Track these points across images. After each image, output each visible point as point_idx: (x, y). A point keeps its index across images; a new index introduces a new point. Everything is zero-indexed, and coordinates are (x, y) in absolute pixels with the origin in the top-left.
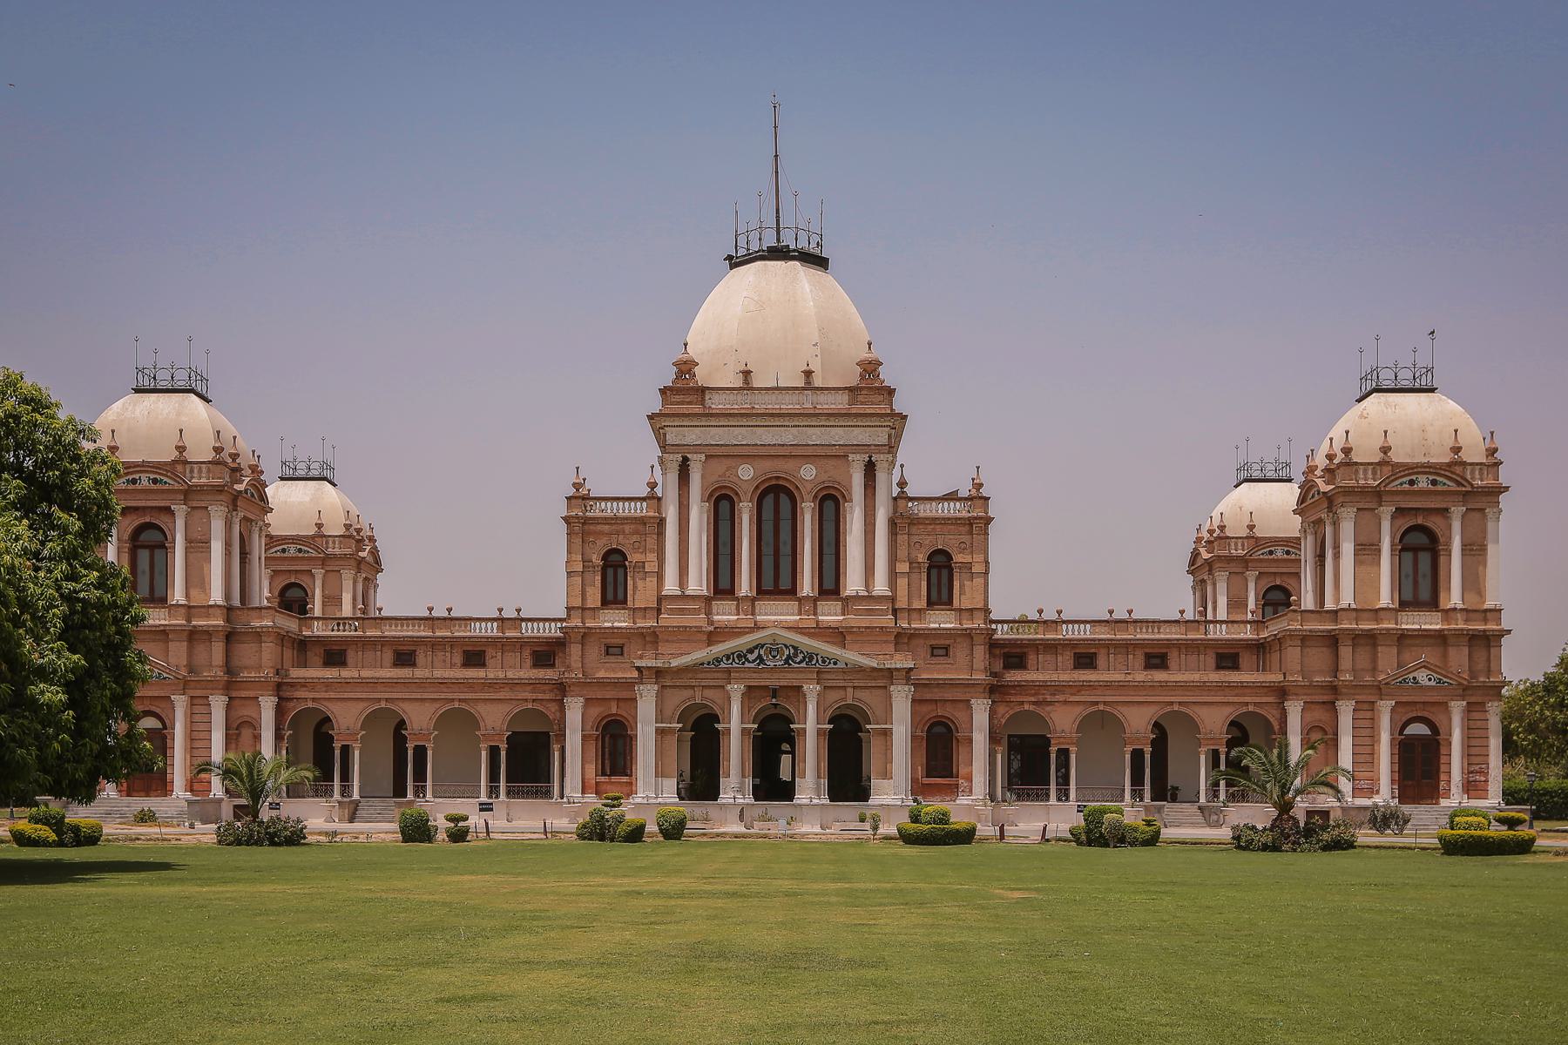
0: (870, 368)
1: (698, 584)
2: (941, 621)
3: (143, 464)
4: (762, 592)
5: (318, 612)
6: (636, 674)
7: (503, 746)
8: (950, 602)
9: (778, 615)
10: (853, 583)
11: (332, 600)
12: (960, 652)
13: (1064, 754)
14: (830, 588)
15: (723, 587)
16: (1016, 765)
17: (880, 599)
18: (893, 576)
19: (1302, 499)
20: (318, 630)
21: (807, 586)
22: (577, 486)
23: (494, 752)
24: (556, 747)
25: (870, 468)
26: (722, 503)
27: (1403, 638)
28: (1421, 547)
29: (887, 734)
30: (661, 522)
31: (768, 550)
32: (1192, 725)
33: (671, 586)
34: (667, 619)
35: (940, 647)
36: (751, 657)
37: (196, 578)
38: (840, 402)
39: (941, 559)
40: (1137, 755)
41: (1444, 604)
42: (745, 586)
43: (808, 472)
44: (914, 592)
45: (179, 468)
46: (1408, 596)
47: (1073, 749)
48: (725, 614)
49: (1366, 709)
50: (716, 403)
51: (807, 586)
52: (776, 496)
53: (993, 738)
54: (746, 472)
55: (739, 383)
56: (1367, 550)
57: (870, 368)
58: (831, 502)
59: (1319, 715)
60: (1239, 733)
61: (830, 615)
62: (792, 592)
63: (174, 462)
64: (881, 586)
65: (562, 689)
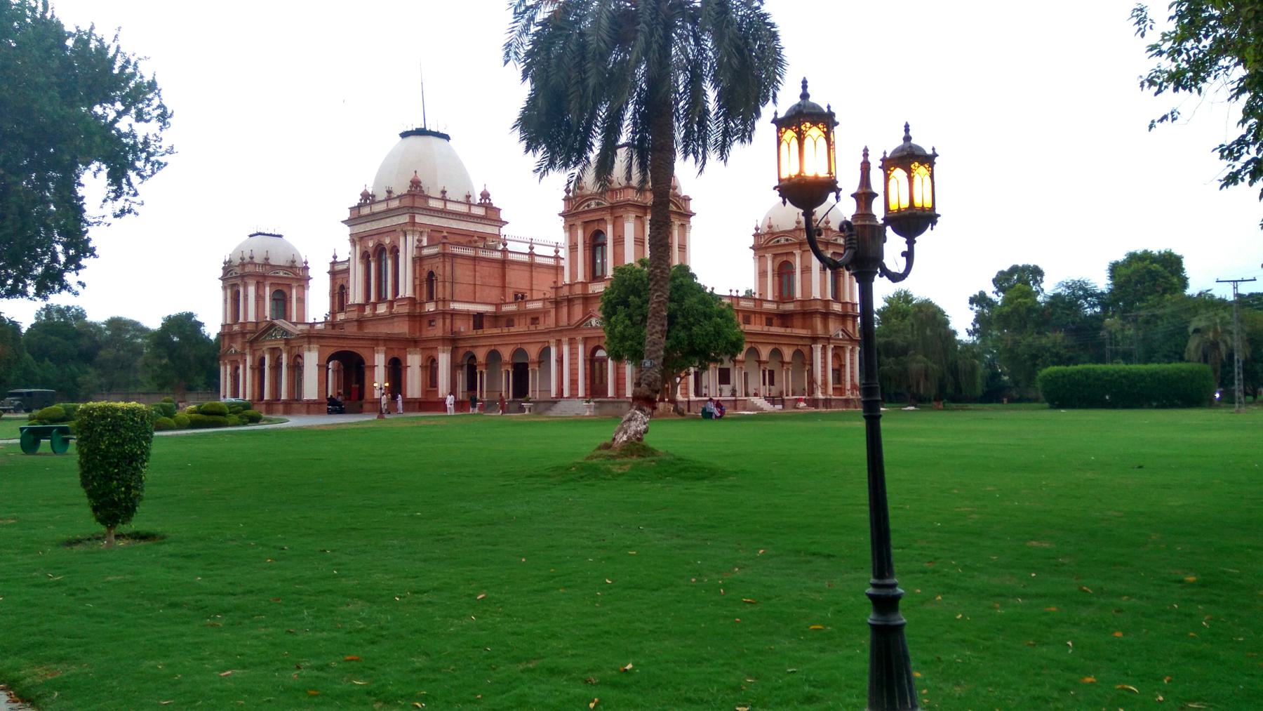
0: (416, 183)
2: (430, 307)
9: (382, 309)
22: (335, 257)
26: (365, 257)
33: (351, 301)
35: (431, 319)
38: (395, 204)
42: (373, 299)
43: (387, 241)
48: (368, 311)
49: (572, 342)
51: (389, 297)
52: (380, 250)
53: (454, 367)
54: (371, 244)
56: (573, 248)
57: (416, 183)
58: (395, 251)
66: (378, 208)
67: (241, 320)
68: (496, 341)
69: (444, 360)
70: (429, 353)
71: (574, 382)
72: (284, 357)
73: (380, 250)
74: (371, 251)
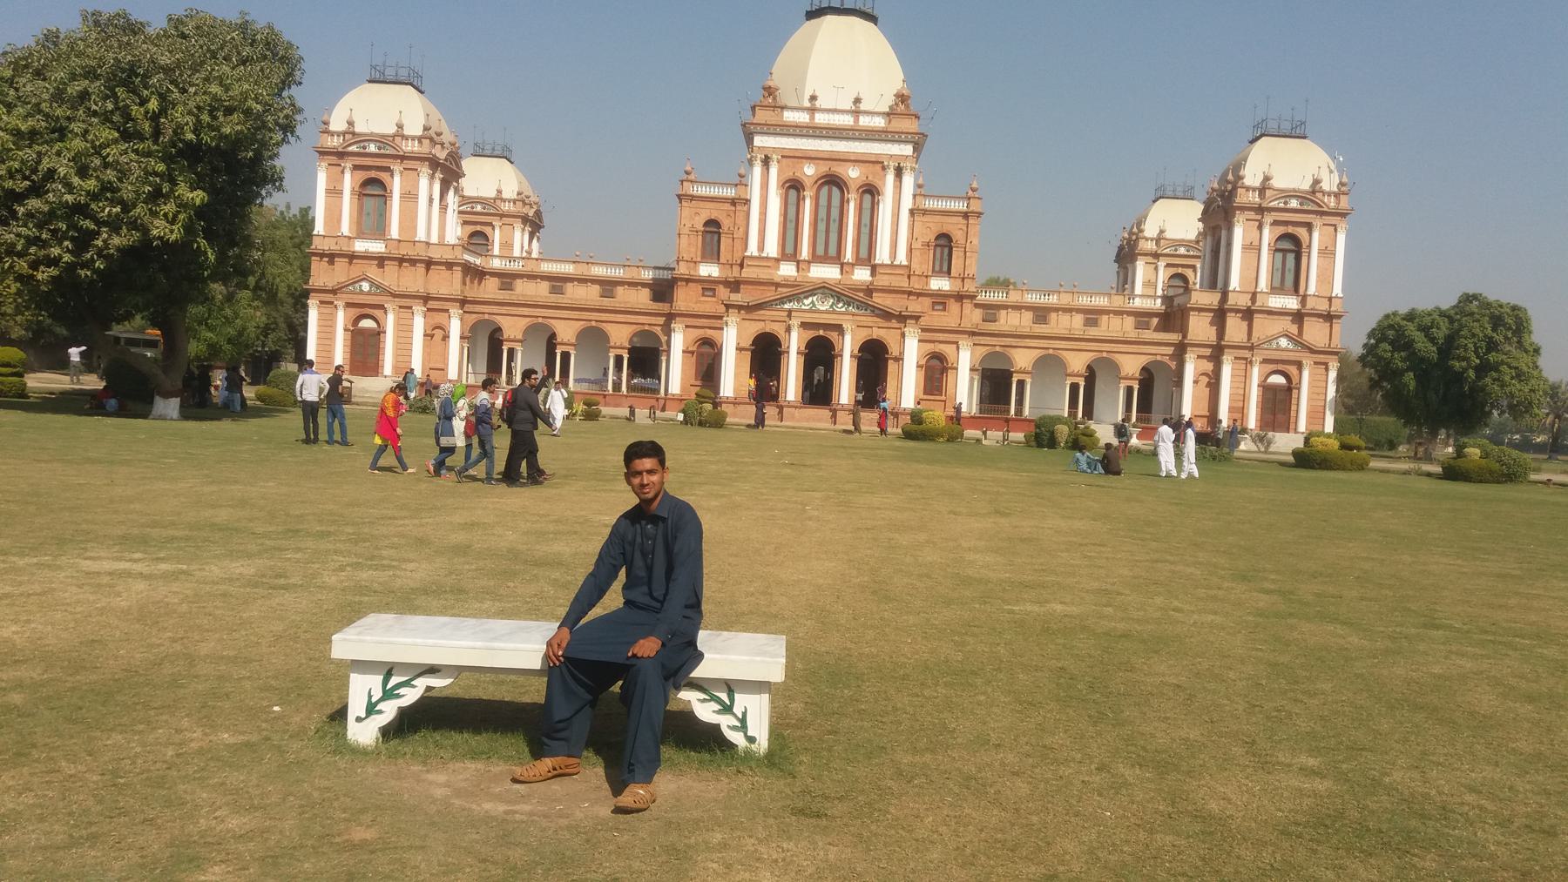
1: (772, 249)
2: (939, 284)
3: (372, 134)
4: (816, 258)
5: (496, 251)
6: (723, 309)
7: (626, 357)
8: (949, 272)
9: (826, 273)
10: (882, 255)
11: (507, 245)
12: (954, 306)
13: (1021, 384)
14: (866, 257)
15: (789, 253)
16: (987, 389)
17: (900, 266)
18: (910, 250)
19: (1205, 213)
20: (496, 264)
21: (849, 256)
23: (619, 359)
24: (664, 358)
25: (899, 172)
27: (1271, 312)
28: (1292, 247)
29: (899, 359)
30: (747, 202)
31: (822, 226)
32: (1113, 367)
34: (747, 273)
36: (806, 302)
37: (409, 219)
38: (879, 122)
39: (942, 242)
40: (1074, 388)
41: (1301, 292)
42: (805, 253)
43: (853, 173)
44: (922, 264)
45: (398, 139)
46: (1277, 284)
47: (1029, 380)
48: (787, 270)
50: (790, 116)
51: (849, 256)
54: (810, 171)
55: (807, 104)
56: (1253, 248)
59: (1208, 366)
60: (1147, 379)
61: (862, 275)
62: (837, 259)
63: (394, 136)
64: (902, 258)
65: (670, 317)
66: (821, 119)
67: (394, 232)
68: (1058, 344)
69: (965, 360)
70: (930, 347)
71: (1239, 410)
72: (848, 338)
73: (833, 181)
74: (808, 183)
